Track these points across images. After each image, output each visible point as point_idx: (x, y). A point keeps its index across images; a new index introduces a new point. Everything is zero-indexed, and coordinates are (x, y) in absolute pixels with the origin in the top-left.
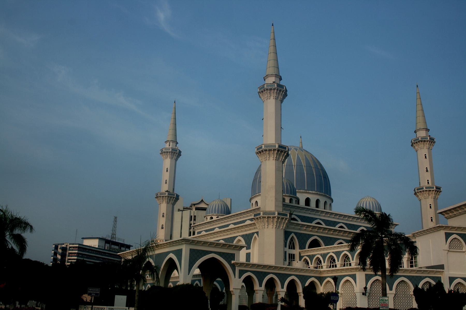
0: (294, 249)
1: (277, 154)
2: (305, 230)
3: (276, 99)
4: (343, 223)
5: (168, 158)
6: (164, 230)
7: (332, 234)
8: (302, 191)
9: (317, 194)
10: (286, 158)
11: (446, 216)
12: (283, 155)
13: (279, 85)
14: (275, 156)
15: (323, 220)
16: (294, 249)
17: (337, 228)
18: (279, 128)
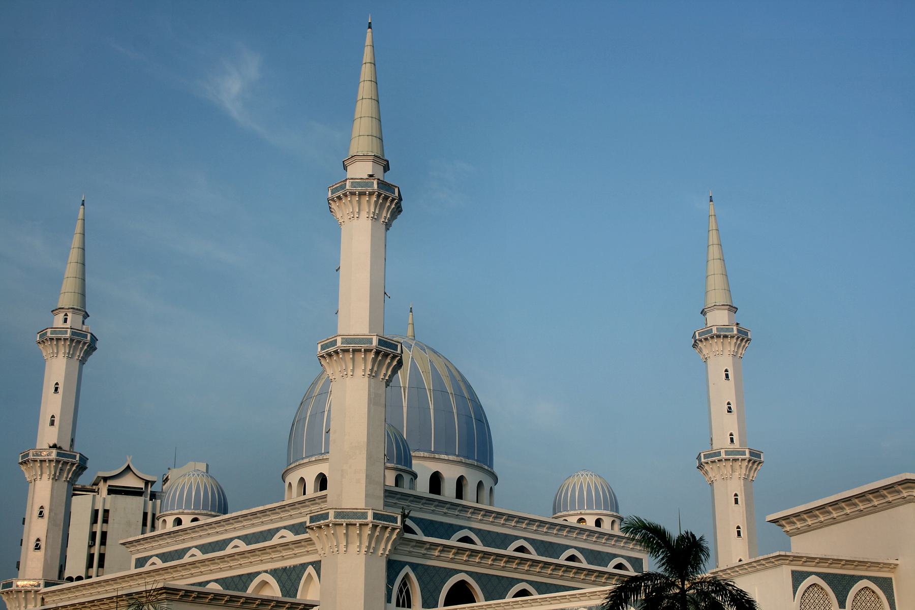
0: (409, 606)
1: (374, 360)
2: (438, 558)
3: (375, 219)
4: (525, 539)
5: (61, 355)
6: (40, 554)
7: (503, 569)
8: (422, 454)
9: (460, 463)
10: (395, 371)
11: (788, 528)
12: (389, 365)
13: (382, 184)
14: (370, 367)
15: (478, 532)
16: (409, 606)
17: (510, 551)
18: (381, 295)
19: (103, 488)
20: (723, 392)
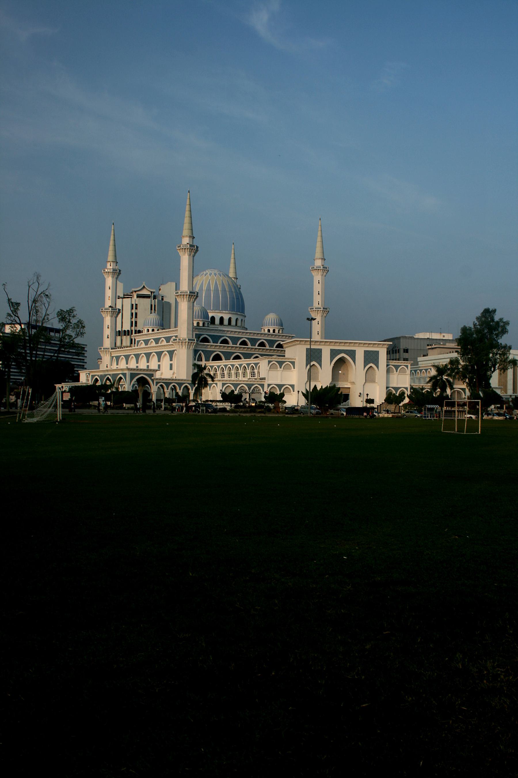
3: (190, 255)
6: (109, 339)
19: (135, 295)
20: (317, 287)
